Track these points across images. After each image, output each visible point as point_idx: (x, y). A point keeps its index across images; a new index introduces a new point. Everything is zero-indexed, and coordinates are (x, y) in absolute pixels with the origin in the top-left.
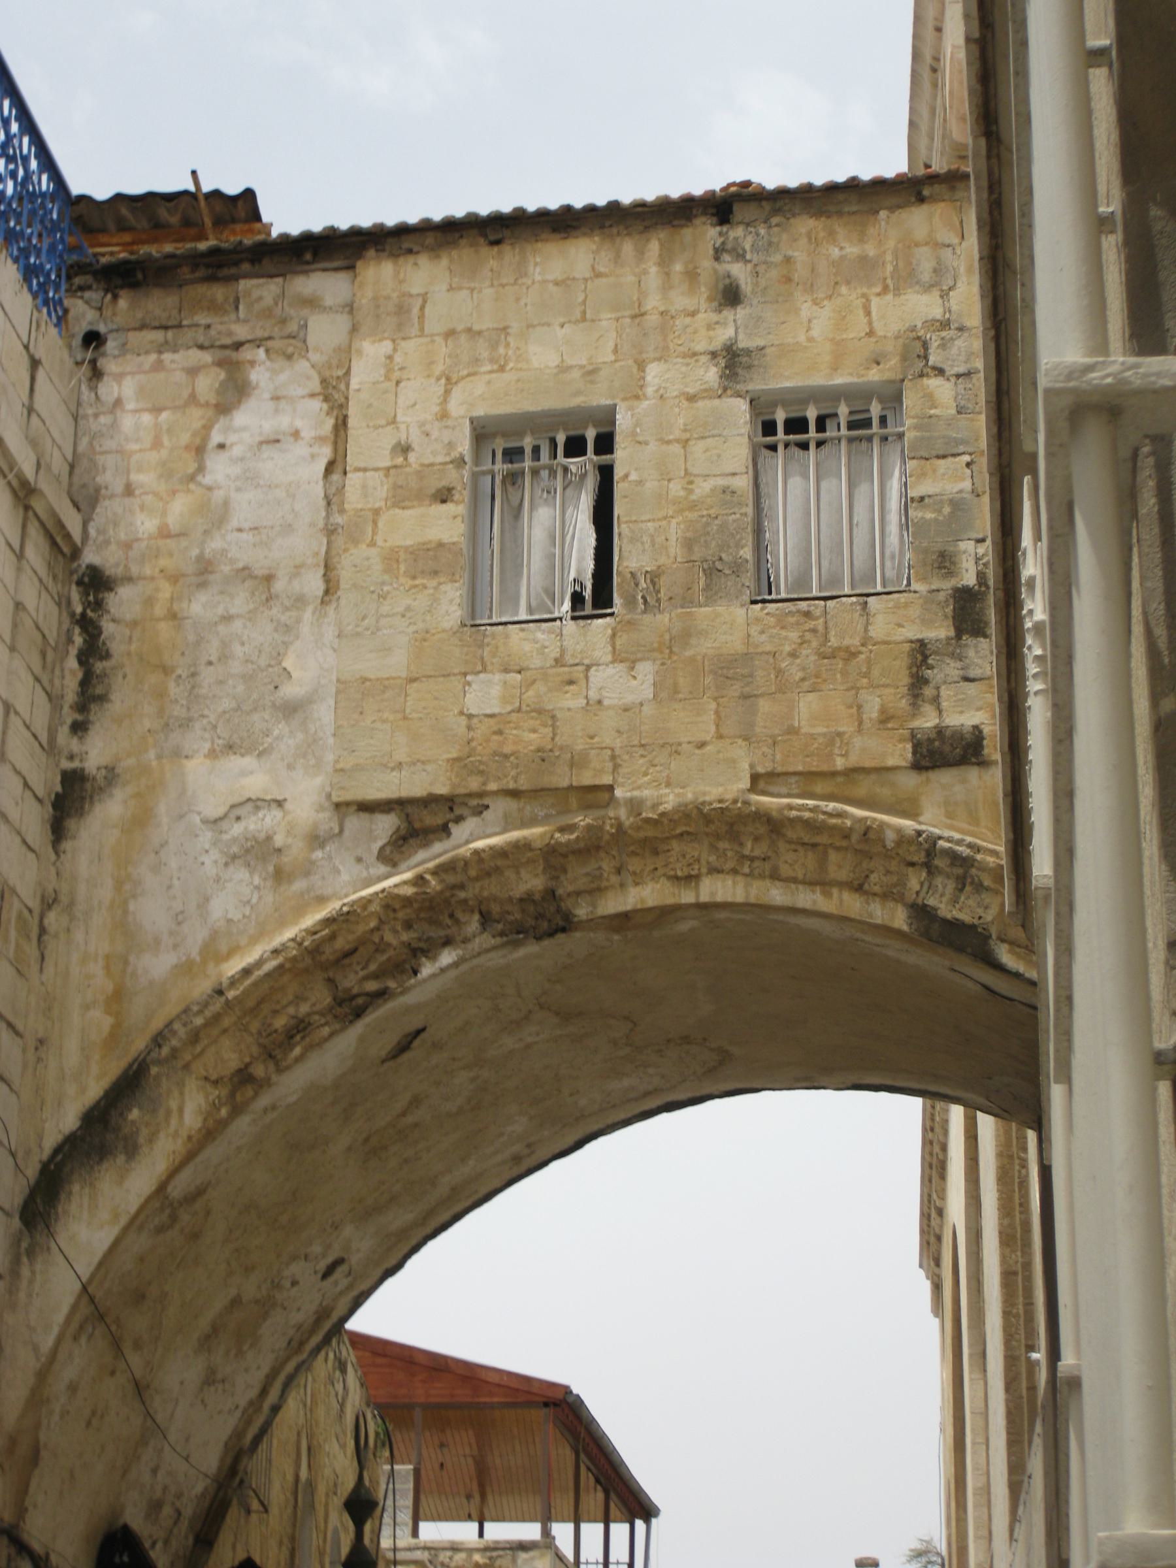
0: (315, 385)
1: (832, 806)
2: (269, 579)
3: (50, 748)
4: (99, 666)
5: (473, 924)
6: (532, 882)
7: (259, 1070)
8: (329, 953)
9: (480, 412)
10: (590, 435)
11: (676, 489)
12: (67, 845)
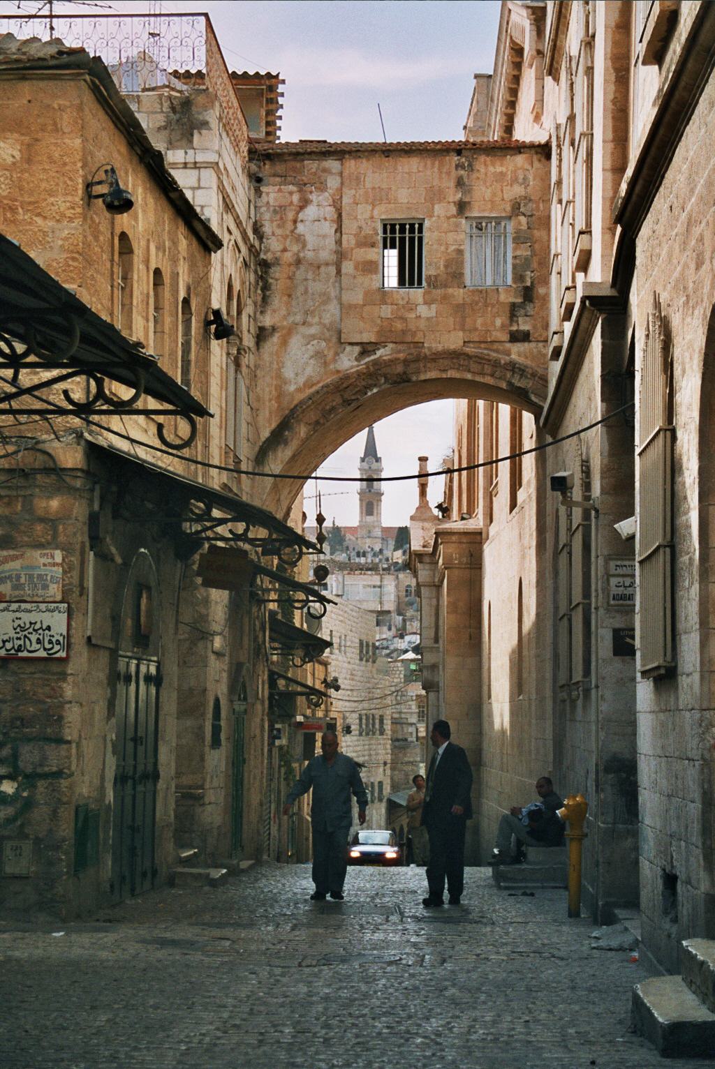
0: (331, 201)
1: (486, 352)
2: (319, 267)
3: (255, 320)
4: (268, 293)
6: (399, 369)
7: (322, 421)
8: (341, 388)
9: (383, 217)
10: (417, 226)
11: (443, 248)
12: (261, 350)
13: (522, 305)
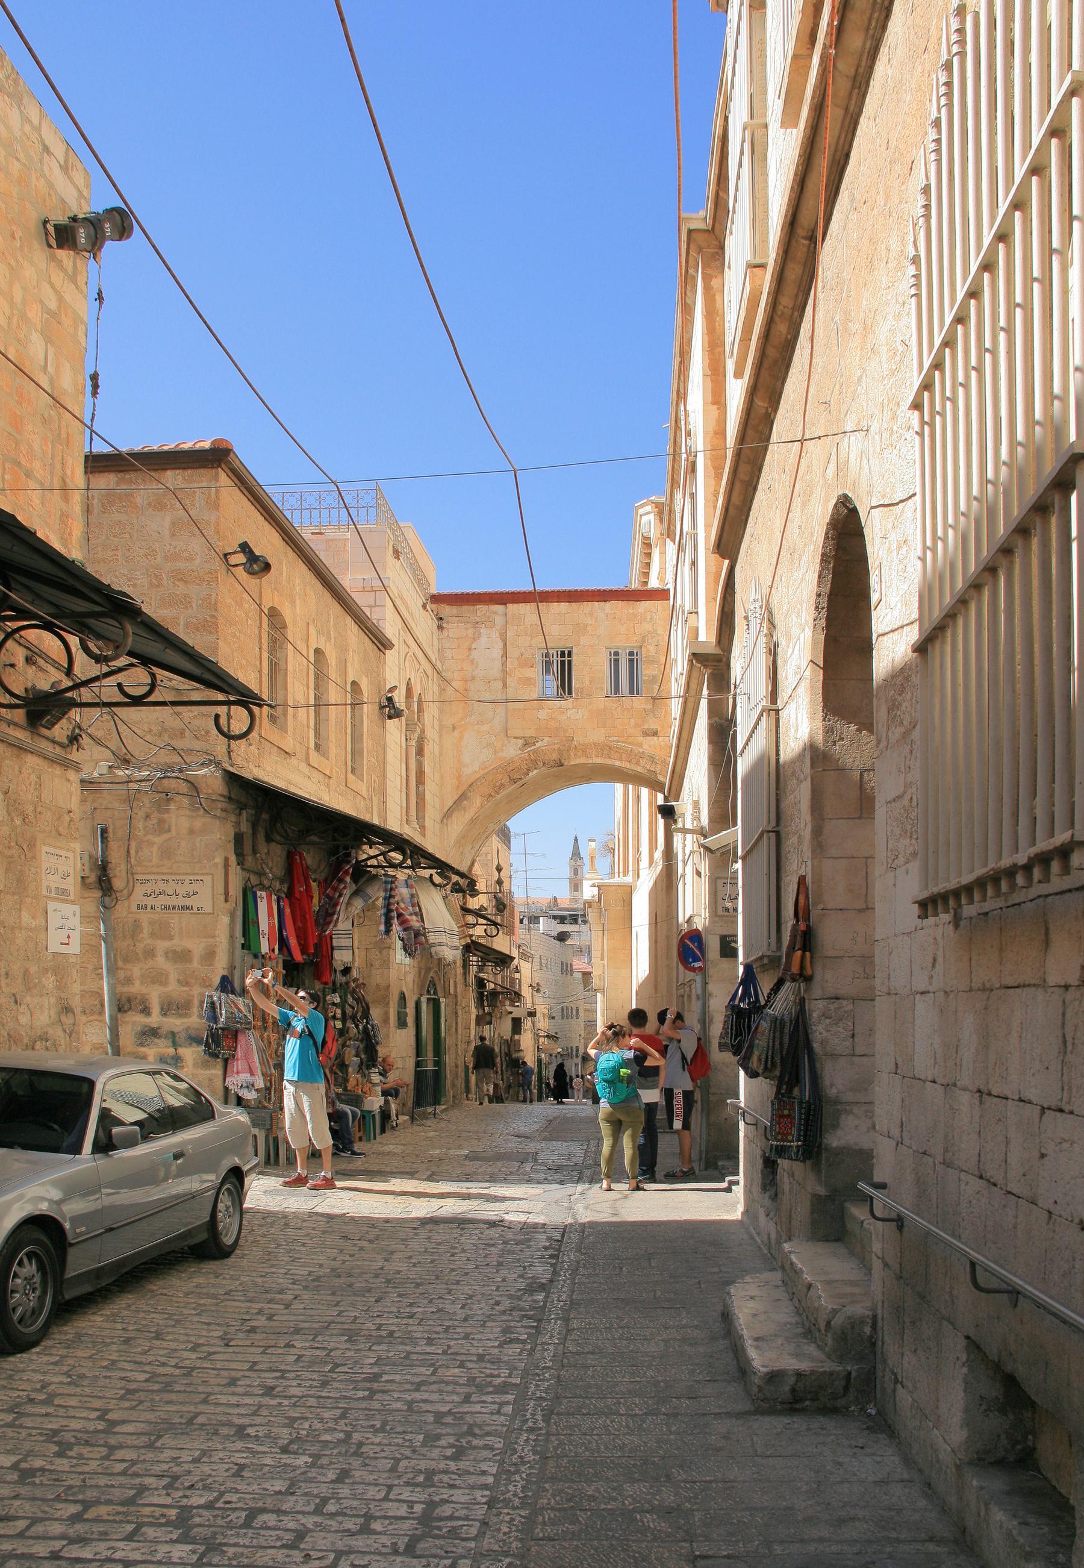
6: (555, 756)
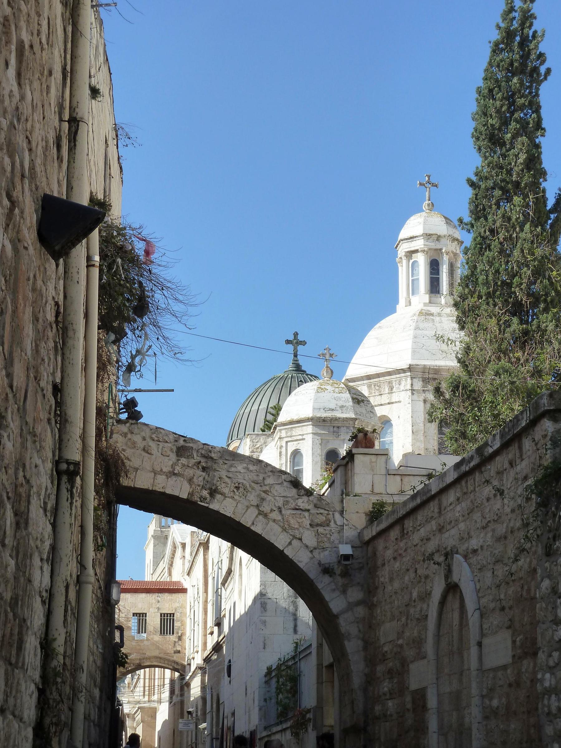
5: (132, 665)
6: (138, 662)
13: (178, 642)
